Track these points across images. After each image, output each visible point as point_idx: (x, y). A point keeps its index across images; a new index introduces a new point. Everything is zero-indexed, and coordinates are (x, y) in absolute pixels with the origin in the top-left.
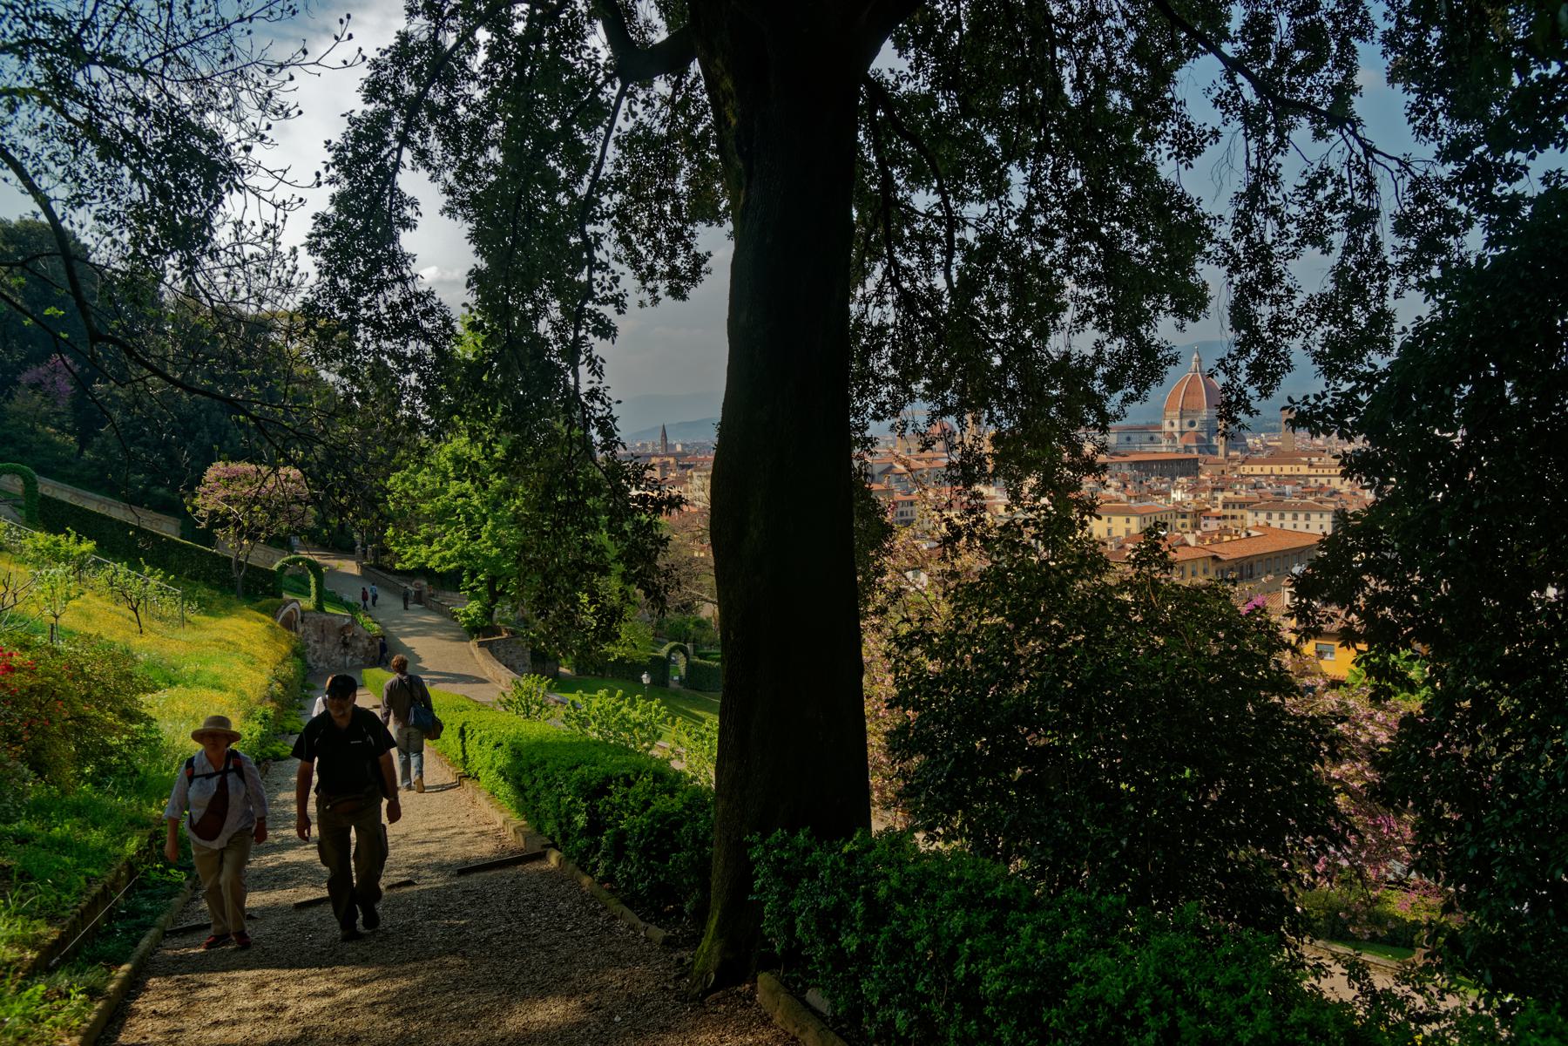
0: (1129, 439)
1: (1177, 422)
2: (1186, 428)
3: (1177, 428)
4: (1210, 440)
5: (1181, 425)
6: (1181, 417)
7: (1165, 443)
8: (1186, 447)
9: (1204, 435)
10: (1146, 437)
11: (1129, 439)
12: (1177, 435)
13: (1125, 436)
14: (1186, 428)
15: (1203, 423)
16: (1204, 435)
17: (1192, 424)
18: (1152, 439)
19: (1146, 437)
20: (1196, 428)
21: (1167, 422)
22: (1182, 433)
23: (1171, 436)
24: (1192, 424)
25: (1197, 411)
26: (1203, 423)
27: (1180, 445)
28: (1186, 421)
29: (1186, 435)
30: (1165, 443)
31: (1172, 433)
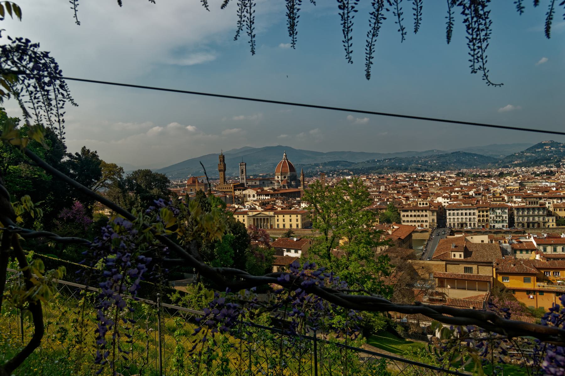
0: (263, 183)
1: (280, 177)
2: (283, 179)
3: (280, 179)
4: (291, 183)
5: (281, 178)
6: (281, 175)
7: (276, 184)
8: (283, 185)
9: (289, 181)
10: (270, 182)
11: (263, 183)
12: (280, 181)
13: (262, 182)
14: (283, 179)
15: (288, 177)
16: (289, 181)
17: (285, 177)
18: (271, 183)
19: (270, 182)
20: (286, 179)
21: (276, 177)
22: (282, 180)
23: (278, 182)
24: (285, 177)
25: (287, 173)
26: (288, 177)
27: (282, 185)
28: (283, 176)
29: (283, 181)
30: (276, 184)
31: (278, 180)
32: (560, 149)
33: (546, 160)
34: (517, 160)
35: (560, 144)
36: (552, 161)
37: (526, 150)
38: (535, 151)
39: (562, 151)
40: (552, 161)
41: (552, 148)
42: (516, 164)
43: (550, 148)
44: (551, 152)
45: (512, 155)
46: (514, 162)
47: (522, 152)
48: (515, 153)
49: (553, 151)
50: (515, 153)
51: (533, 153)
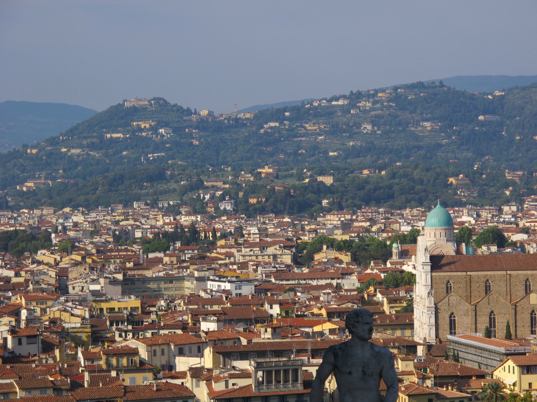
32: (191, 136)
33: (151, 179)
34: (32, 177)
35: (189, 112)
36: (173, 185)
37: (72, 132)
38: (101, 138)
39: (196, 142)
40: (173, 185)
41: (162, 131)
42: (31, 193)
43: (154, 129)
44: (157, 148)
45: (15, 155)
46: (22, 183)
47: (53, 142)
48: (25, 146)
49: (163, 143)
50: (25, 146)
51: (92, 146)
